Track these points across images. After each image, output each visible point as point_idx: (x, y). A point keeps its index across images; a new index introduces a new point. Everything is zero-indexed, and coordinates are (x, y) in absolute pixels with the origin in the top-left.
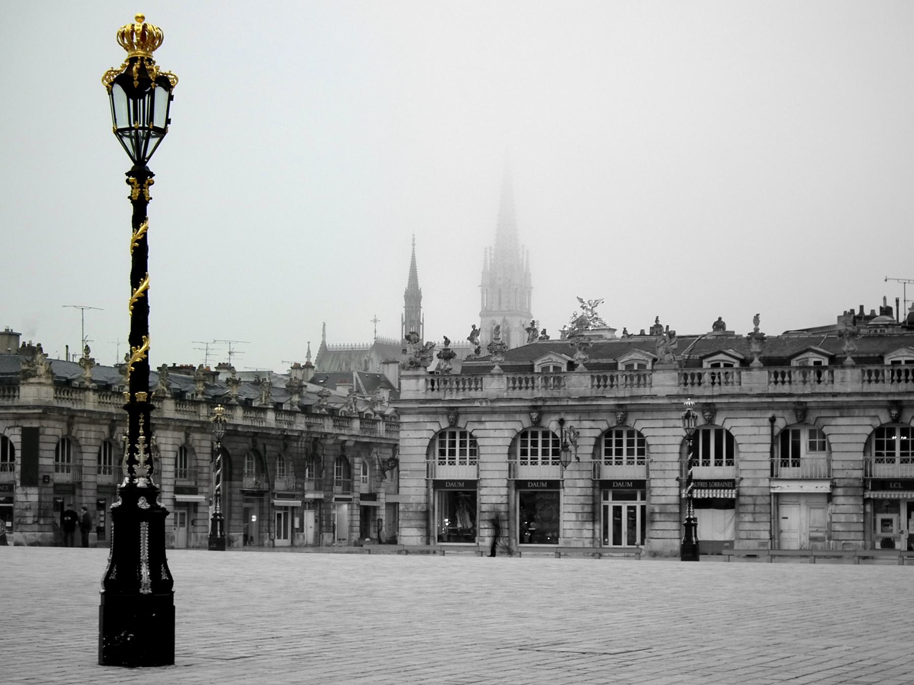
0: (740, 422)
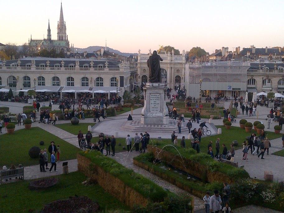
0: (257, 78)
